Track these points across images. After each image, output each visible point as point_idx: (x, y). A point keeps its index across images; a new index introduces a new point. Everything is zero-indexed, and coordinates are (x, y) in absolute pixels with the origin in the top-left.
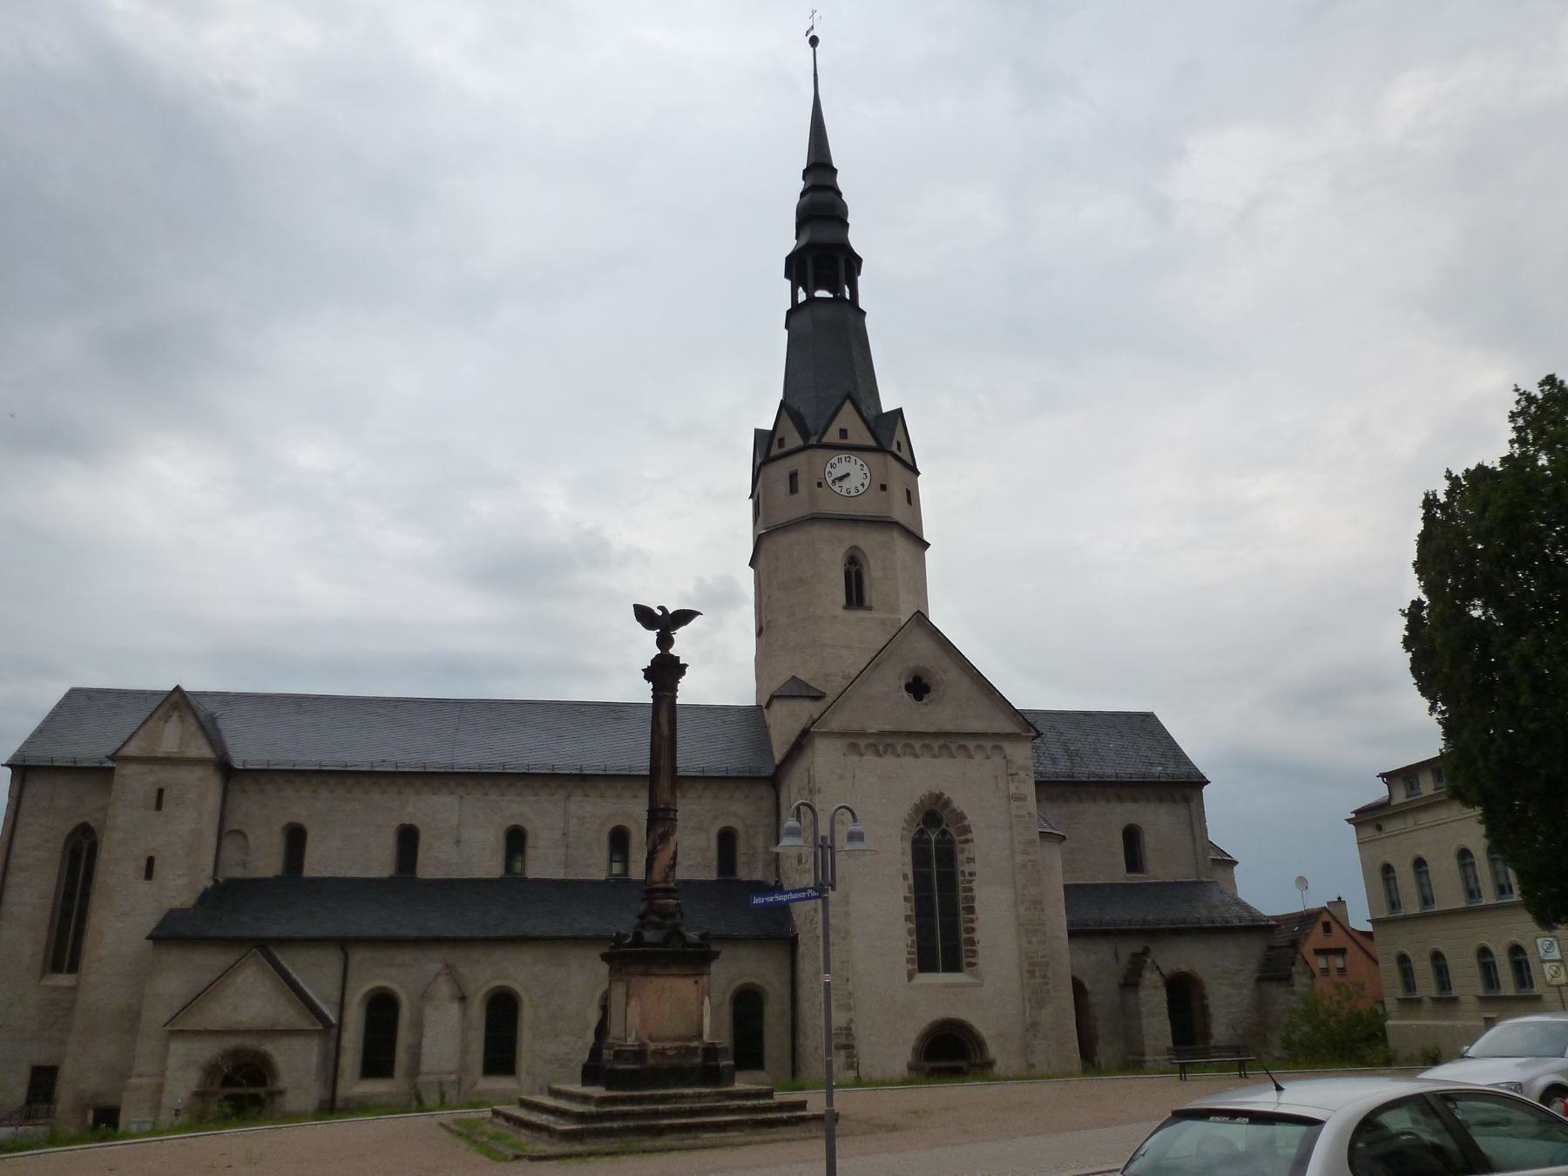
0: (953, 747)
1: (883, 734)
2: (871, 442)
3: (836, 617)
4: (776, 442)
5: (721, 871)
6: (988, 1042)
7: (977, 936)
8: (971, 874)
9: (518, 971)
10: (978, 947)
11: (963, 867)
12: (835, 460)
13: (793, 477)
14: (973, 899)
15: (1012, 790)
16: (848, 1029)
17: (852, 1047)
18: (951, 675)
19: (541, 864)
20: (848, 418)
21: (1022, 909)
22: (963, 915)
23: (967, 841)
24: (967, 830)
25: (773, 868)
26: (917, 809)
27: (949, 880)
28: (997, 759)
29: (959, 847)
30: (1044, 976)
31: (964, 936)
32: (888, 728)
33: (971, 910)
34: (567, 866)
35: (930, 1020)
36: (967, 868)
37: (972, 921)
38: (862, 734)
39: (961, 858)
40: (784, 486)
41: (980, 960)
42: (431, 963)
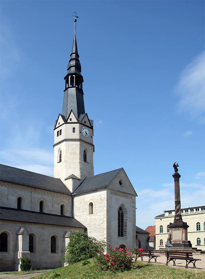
4: (69, 119)
5: (61, 214)
8: (127, 220)
9: (35, 229)
12: (83, 128)
13: (74, 129)
22: (124, 227)
23: (126, 214)
33: (126, 226)
36: (126, 219)
38: (113, 190)
39: (125, 217)
41: (127, 235)
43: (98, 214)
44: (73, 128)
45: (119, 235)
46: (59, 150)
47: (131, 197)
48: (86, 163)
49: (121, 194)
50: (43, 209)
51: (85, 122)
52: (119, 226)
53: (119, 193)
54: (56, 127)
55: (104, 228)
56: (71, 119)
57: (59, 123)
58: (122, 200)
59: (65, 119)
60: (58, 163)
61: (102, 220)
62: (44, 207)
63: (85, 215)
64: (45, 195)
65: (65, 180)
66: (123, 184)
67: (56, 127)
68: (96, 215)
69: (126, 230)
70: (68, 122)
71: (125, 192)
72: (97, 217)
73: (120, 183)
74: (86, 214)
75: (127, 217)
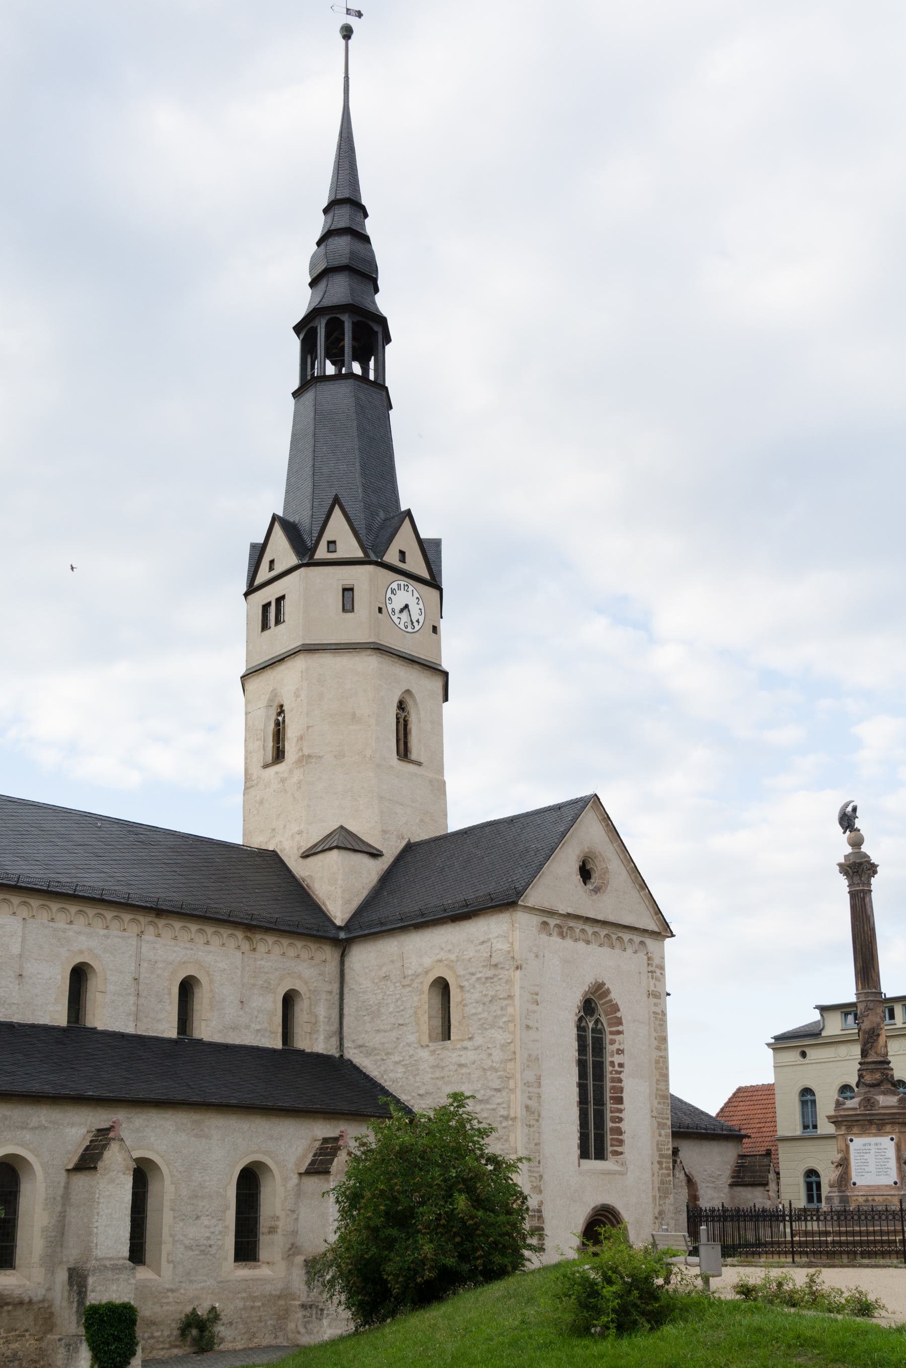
0: (614, 937)
1: (569, 916)
2: (426, 575)
3: (392, 767)
7: (624, 1126)
8: (621, 1065)
10: (624, 1137)
11: (611, 1057)
13: (348, 591)
14: (621, 1090)
15: (652, 988)
16: (540, 1211)
17: (542, 1229)
18: (615, 865)
19: (108, 1014)
20: (403, 540)
21: (656, 1102)
22: (609, 1105)
23: (619, 1033)
24: (619, 1022)
25: (334, 1041)
26: (586, 993)
27: (599, 1067)
28: (642, 956)
29: (609, 1037)
32: (570, 911)
33: (620, 1100)
34: (137, 1019)
35: (593, 1206)
36: (617, 1059)
37: (621, 1111)
38: (552, 913)
39: (610, 1048)
40: (336, 599)
42: (74, 1128)
43: (479, 1040)
44: (345, 590)
45: (584, 1154)
46: (271, 700)
47: (642, 943)
48: (412, 768)
49: (590, 930)
50: (196, 1024)
51: (402, 553)
52: (583, 1101)
53: (578, 926)
54: (257, 582)
55: (506, 1118)
56: (331, 543)
57: (272, 562)
58: (598, 963)
59: (303, 542)
60: (266, 766)
61: (496, 1071)
62: (197, 1006)
63: (409, 1045)
64: (208, 943)
65: (306, 856)
66: (595, 880)
67: (257, 582)
68: (468, 1044)
69: (621, 1120)
70: (316, 557)
71: (611, 918)
72: (470, 1056)
73: (585, 873)
74: (412, 1038)
75: (627, 1049)
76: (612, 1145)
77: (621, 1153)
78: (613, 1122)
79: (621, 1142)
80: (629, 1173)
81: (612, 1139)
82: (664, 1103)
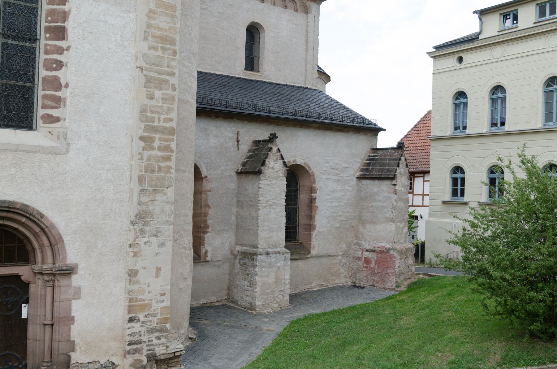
6: (66, 239)
14: (65, 16)
22: (44, 41)
30: (167, 148)
31: (42, 73)
33: (60, 33)
37: (60, 51)
69: (60, 65)
76: (44, 107)
77: (58, 120)
78: (47, 69)
79: (58, 102)
80: (72, 153)
81: (44, 97)
82: (164, 49)
